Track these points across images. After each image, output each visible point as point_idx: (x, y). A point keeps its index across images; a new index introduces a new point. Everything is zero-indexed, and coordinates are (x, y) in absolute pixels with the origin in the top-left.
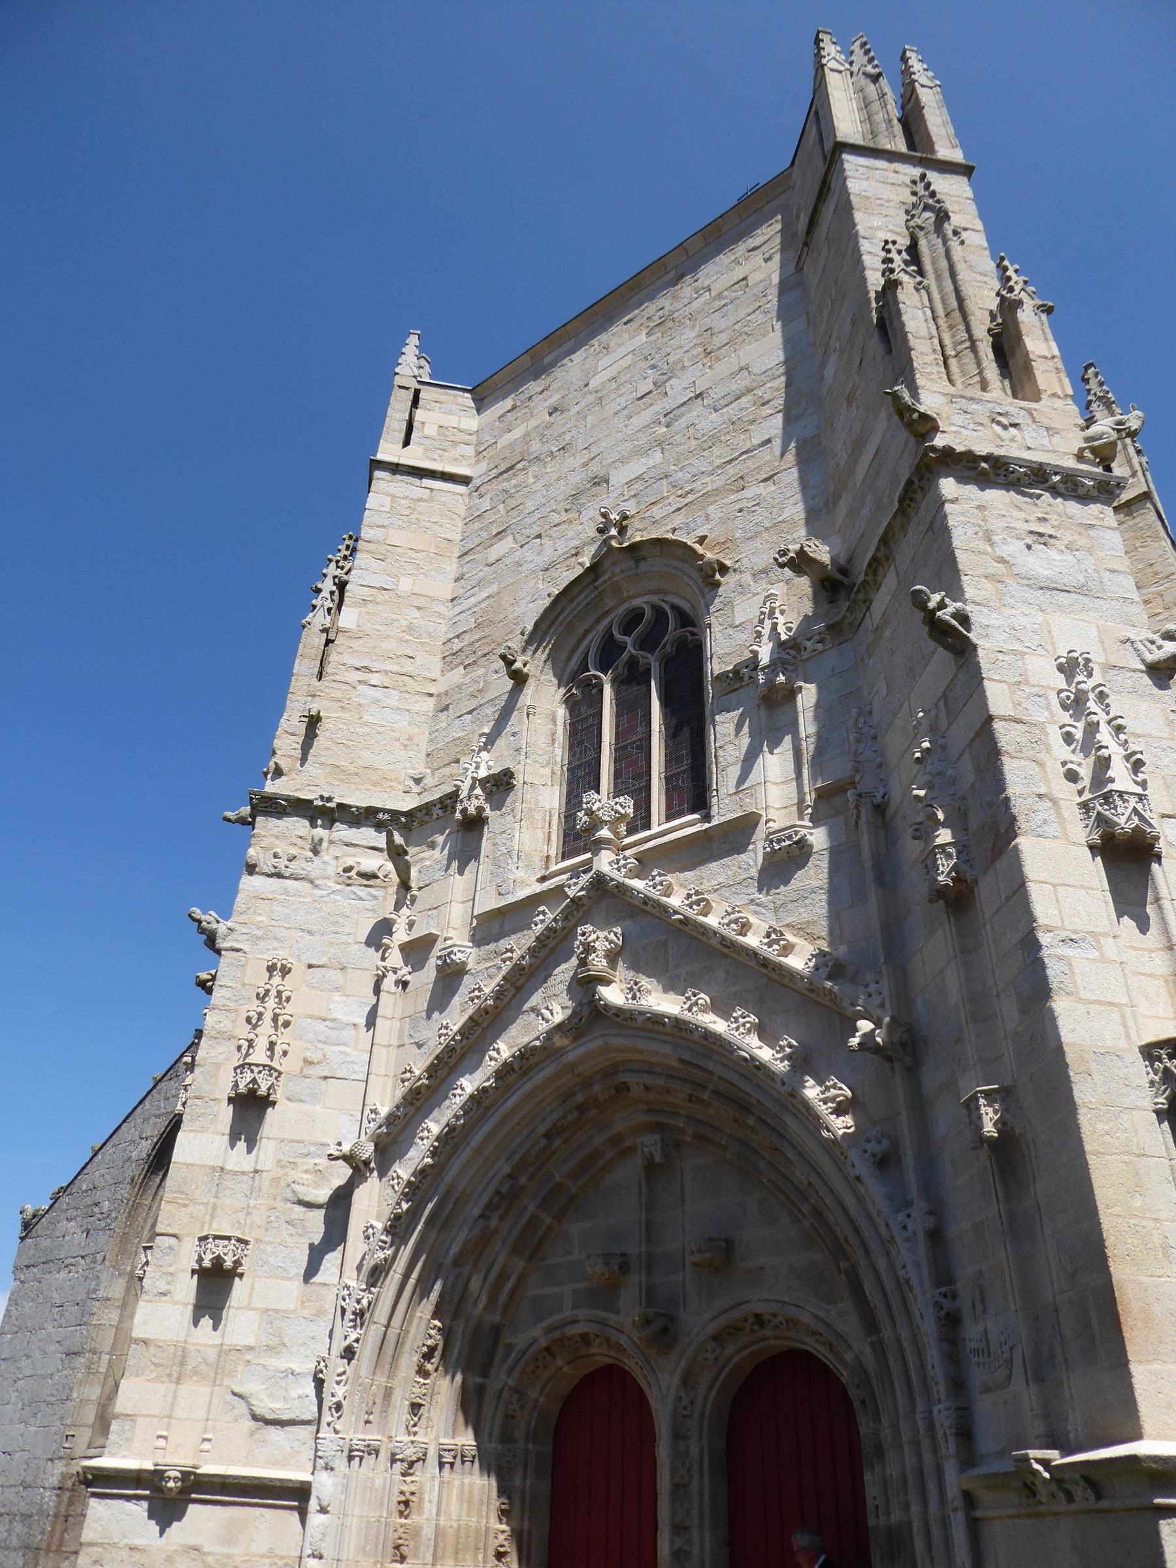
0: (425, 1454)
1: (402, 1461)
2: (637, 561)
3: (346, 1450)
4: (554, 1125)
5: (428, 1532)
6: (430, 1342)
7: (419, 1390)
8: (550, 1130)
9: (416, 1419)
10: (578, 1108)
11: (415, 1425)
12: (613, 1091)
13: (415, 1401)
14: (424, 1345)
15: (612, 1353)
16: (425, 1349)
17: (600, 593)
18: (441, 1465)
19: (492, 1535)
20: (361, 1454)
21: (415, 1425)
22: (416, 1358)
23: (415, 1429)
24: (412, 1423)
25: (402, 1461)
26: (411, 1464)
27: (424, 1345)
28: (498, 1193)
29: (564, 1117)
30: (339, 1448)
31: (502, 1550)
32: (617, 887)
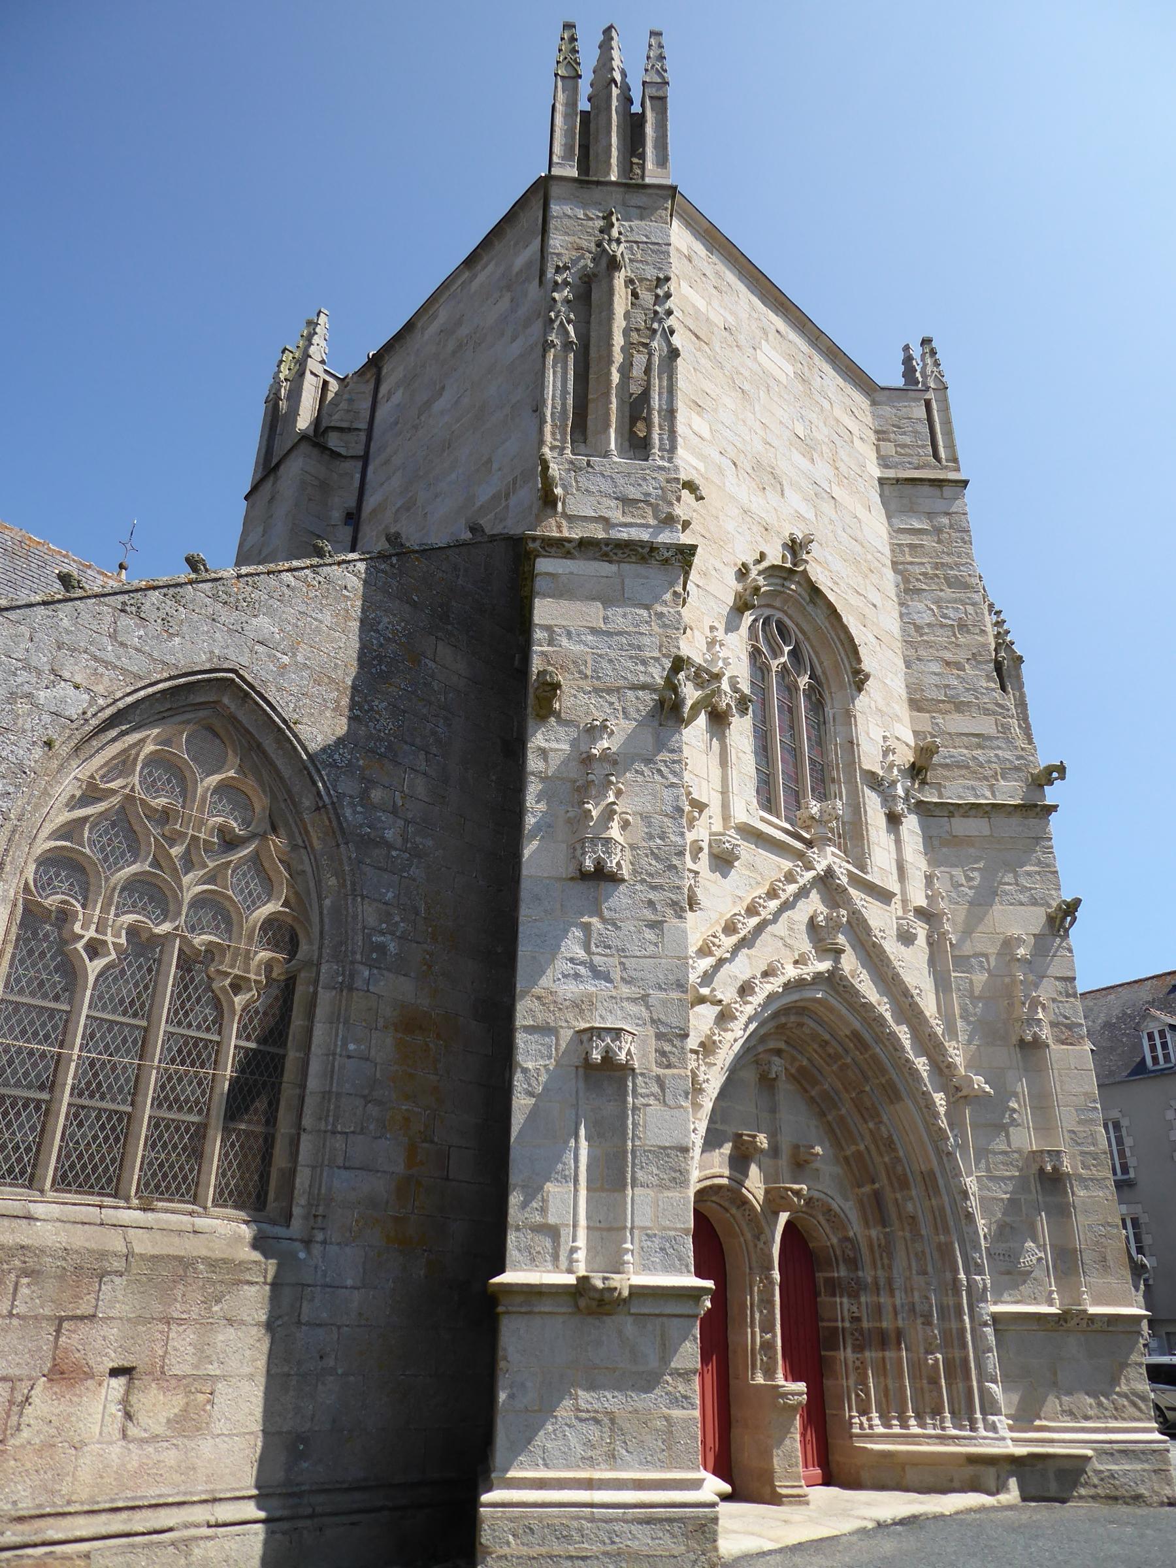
2: (812, 601)
17: (781, 592)
32: (838, 885)
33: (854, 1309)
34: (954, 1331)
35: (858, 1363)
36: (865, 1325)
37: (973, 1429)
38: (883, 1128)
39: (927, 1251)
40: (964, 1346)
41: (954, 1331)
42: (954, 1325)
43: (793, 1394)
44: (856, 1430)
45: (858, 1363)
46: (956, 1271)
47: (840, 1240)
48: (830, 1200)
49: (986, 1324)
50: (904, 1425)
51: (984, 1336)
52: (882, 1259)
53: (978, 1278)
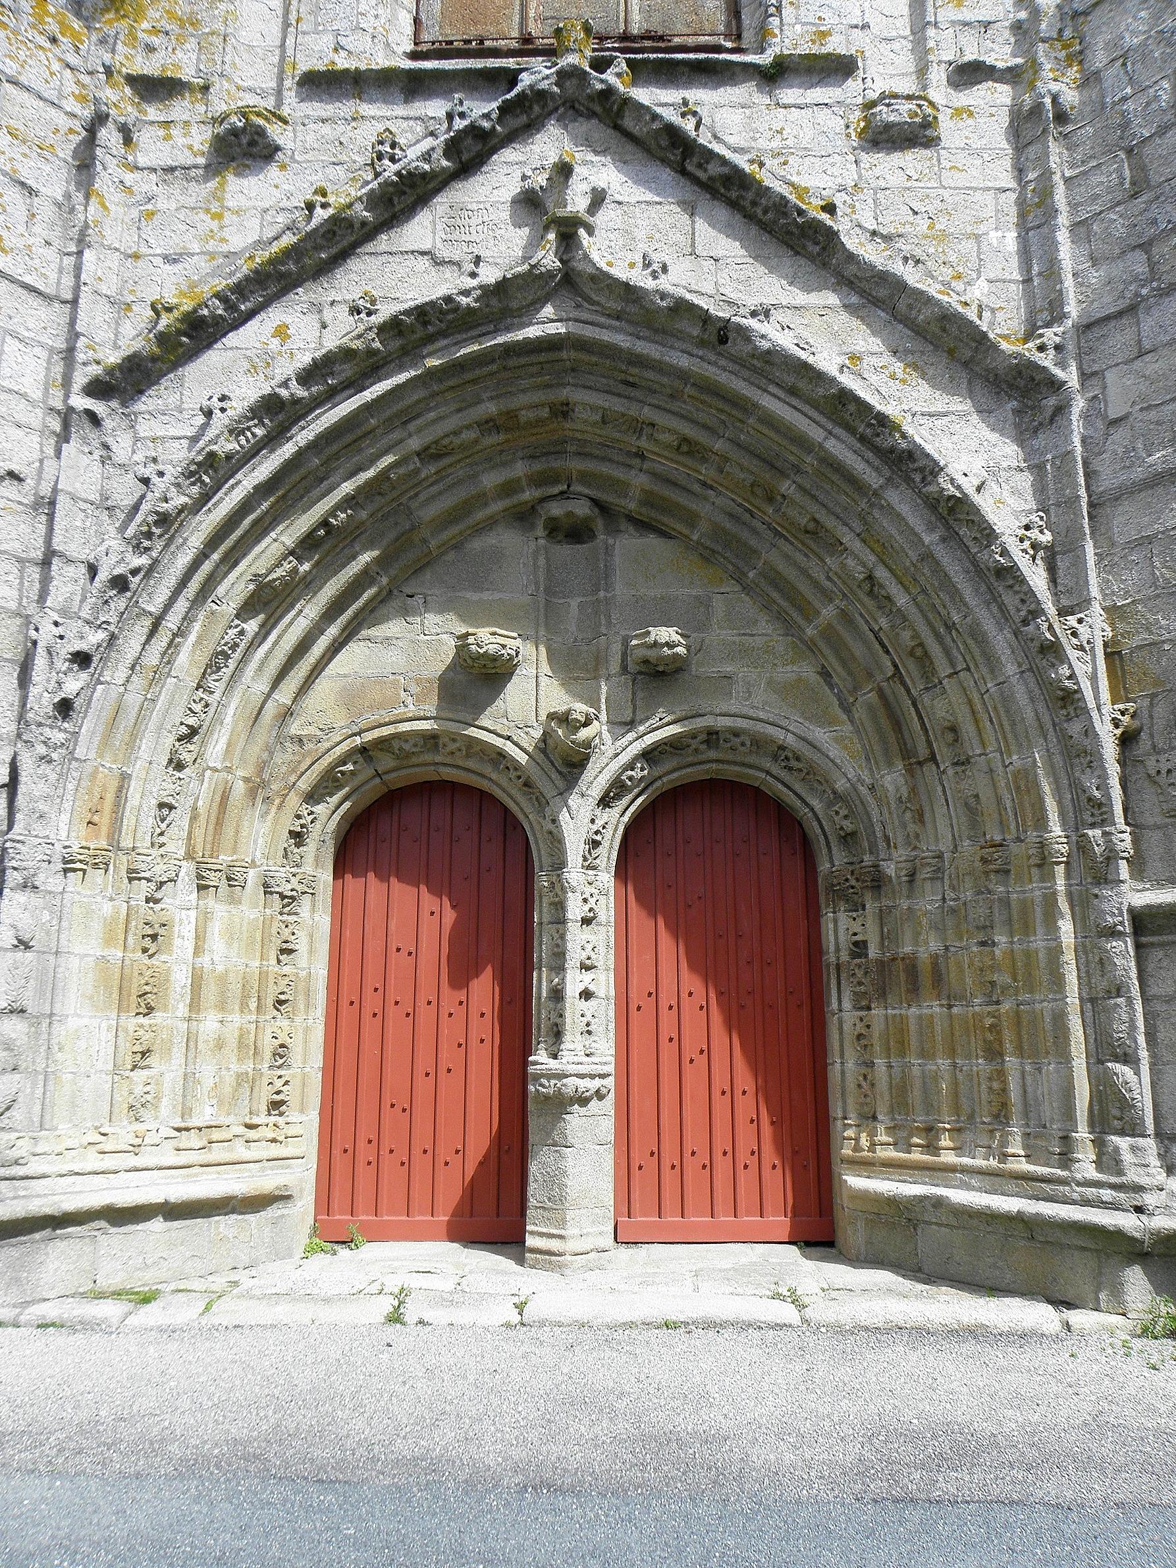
0: (177, 875)
1: (149, 880)
3: (57, 858)
4: (436, 442)
5: (181, 978)
6: (191, 721)
7: (172, 786)
8: (427, 448)
9: (163, 826)
10: (479, 424)
11: (162, 834)
12: (545, 413)
13: (165, 800)
14: (182, 724)
15: (470, 764)
16: (184, 730)
18: (201, 888)
19: (271, 981)
20: (85, 867)
21: (162, 834)
22: (169, 740)
23: (162, 839)
24: (158, 831)
25: (149, 880)
26: (162, 883)
27: (182, 724)
28: (324, 523)
29: (456, 433)
30: (46, 858)
31: (282, 997)
33: (858, 929)
34: (1042, 955)
35: (860, 1028)
36: (873, 952)
37: (1066, 1159)
38: (851, 562)
39: (986, 795)
40: (1058, 982)
41: (1042, 955)
42: (1039, 942)
43: (550, 1077)
44: (847, 1152)
45: (860, 1028)
46: (1041, 822)
47: (830, 804)
48: (771, 730)
49: (1113, 933)
50: (932, 1148)
51: (1104, 963)
52: (904, 826)
53: (1095, 833)
